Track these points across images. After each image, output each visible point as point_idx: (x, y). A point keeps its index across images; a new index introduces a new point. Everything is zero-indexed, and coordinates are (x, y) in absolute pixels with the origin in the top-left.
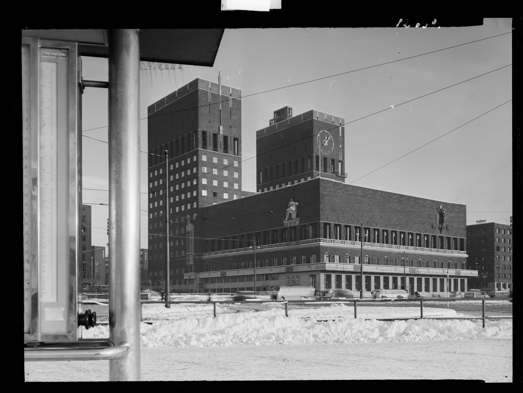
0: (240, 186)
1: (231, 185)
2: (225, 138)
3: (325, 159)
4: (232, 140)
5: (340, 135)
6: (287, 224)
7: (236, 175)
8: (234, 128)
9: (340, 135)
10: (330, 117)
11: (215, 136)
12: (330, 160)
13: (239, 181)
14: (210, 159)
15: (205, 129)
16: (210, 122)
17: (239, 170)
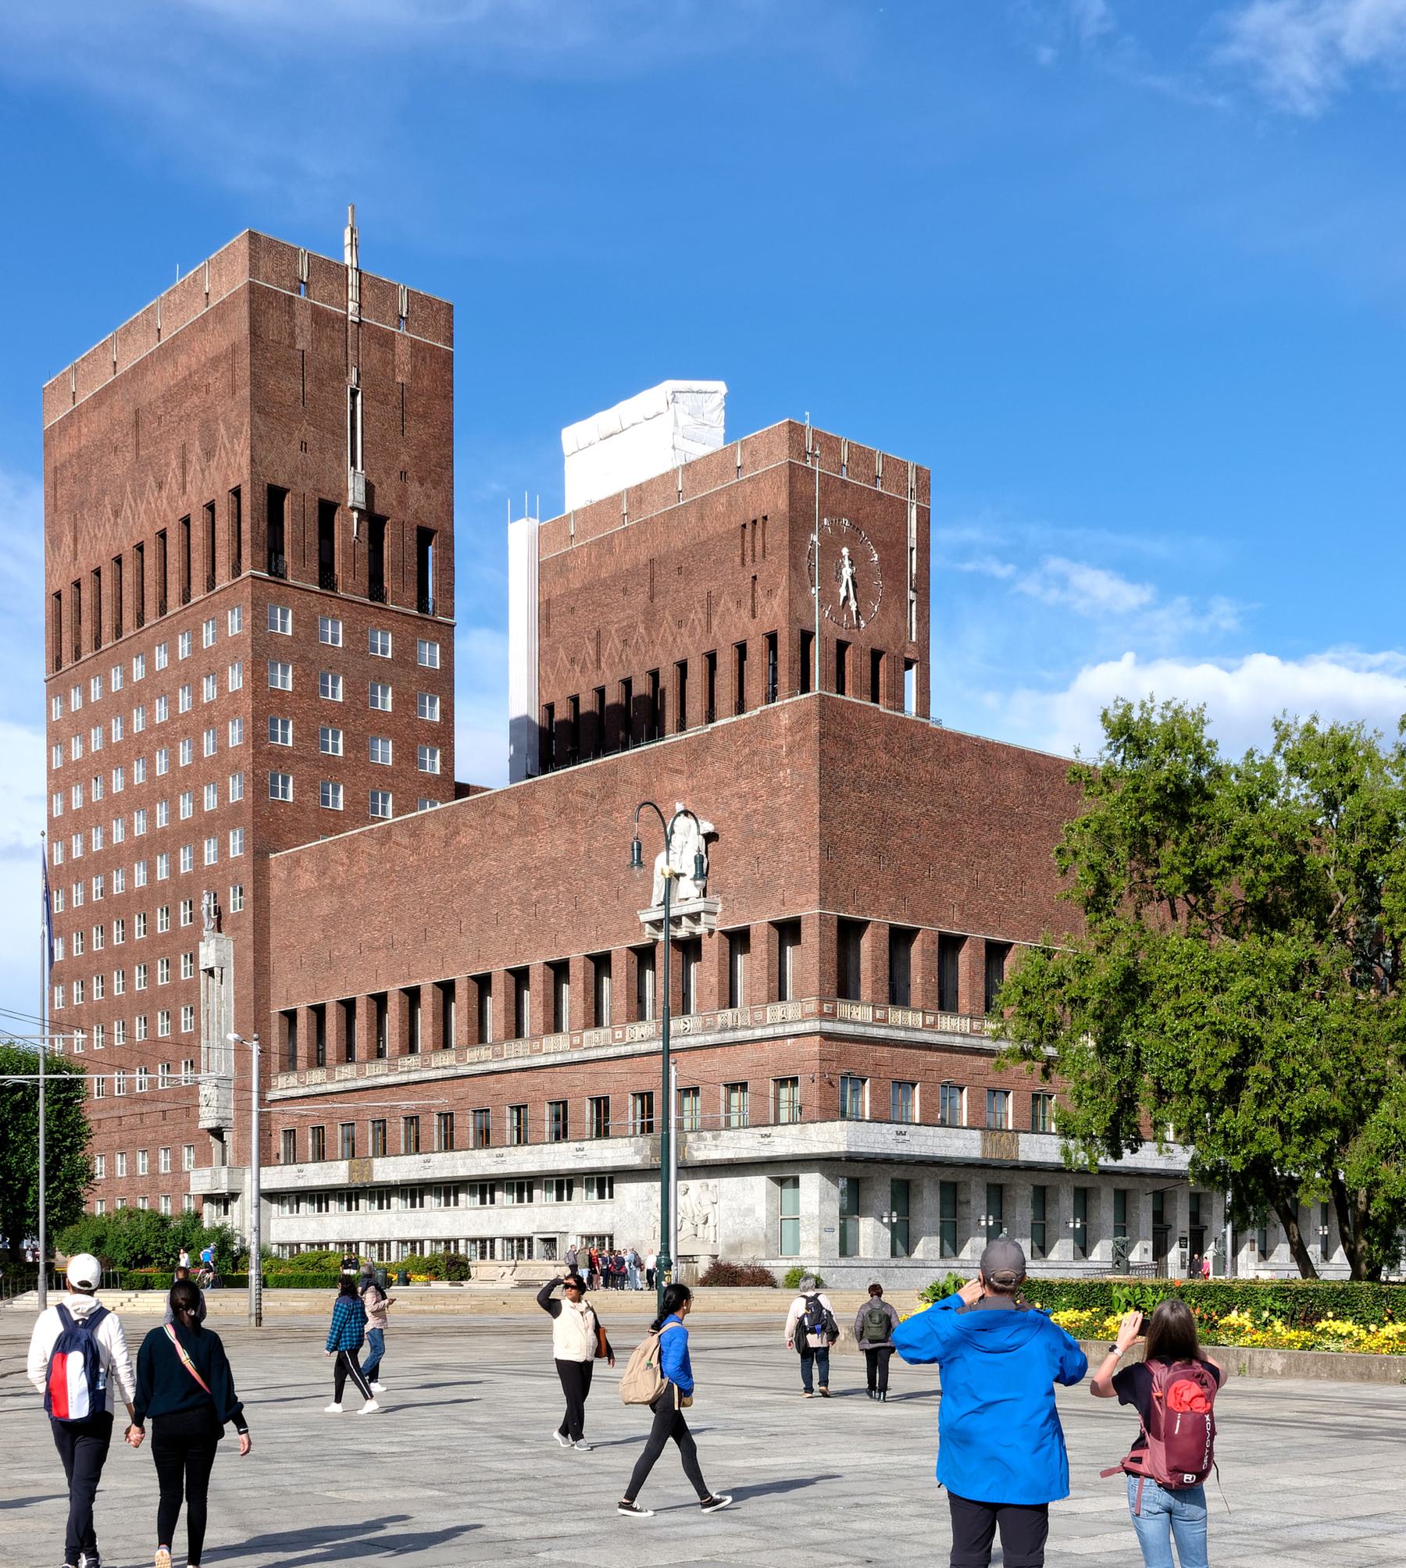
5: (912, 542)
9: (912, 542)
13: (443, 736)
17: (443, 683)
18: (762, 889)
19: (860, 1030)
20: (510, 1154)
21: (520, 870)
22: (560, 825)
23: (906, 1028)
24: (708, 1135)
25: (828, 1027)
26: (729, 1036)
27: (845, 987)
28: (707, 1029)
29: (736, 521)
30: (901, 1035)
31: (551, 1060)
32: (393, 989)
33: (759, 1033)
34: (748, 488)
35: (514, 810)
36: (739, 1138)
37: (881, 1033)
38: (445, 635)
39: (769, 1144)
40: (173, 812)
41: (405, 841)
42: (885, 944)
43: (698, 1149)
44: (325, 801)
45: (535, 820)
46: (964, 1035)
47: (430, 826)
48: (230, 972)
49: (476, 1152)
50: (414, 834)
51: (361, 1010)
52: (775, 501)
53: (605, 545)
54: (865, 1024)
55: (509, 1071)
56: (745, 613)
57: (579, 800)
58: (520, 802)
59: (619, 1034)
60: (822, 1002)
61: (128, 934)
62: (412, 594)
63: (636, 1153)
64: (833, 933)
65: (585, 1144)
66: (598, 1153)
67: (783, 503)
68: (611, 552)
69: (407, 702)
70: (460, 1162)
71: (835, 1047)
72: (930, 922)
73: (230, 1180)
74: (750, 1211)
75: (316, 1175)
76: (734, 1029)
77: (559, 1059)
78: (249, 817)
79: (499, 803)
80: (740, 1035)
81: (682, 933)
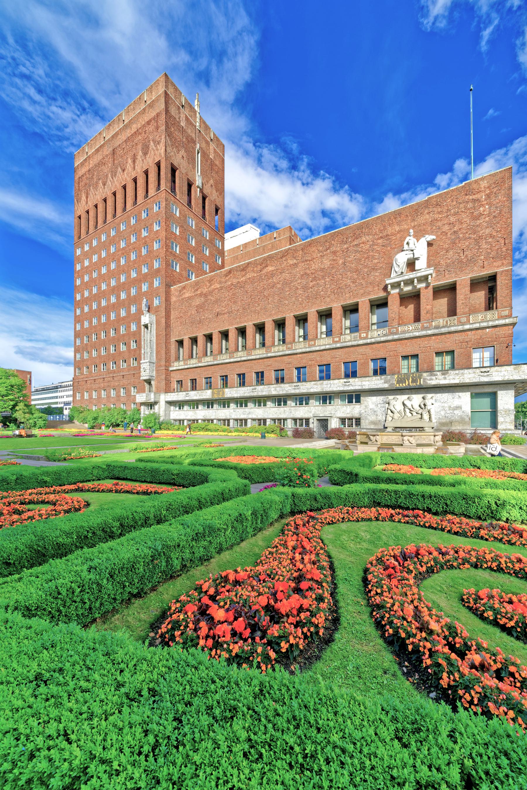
18: (461, 265)
20: (303, 385)
21: (302, 275)
22: (327, 254)
26: (443, 330)
31: (323, 348)
36: (463, 374)
39: (488, 375)
43: (431, 379)
55: (296, 354)
58: (302, 250)
63: (385, 383)
66: (360, 383)
70: (273, 389)
73: (155, 397)
75: (194, 395)
77: (328, 347)
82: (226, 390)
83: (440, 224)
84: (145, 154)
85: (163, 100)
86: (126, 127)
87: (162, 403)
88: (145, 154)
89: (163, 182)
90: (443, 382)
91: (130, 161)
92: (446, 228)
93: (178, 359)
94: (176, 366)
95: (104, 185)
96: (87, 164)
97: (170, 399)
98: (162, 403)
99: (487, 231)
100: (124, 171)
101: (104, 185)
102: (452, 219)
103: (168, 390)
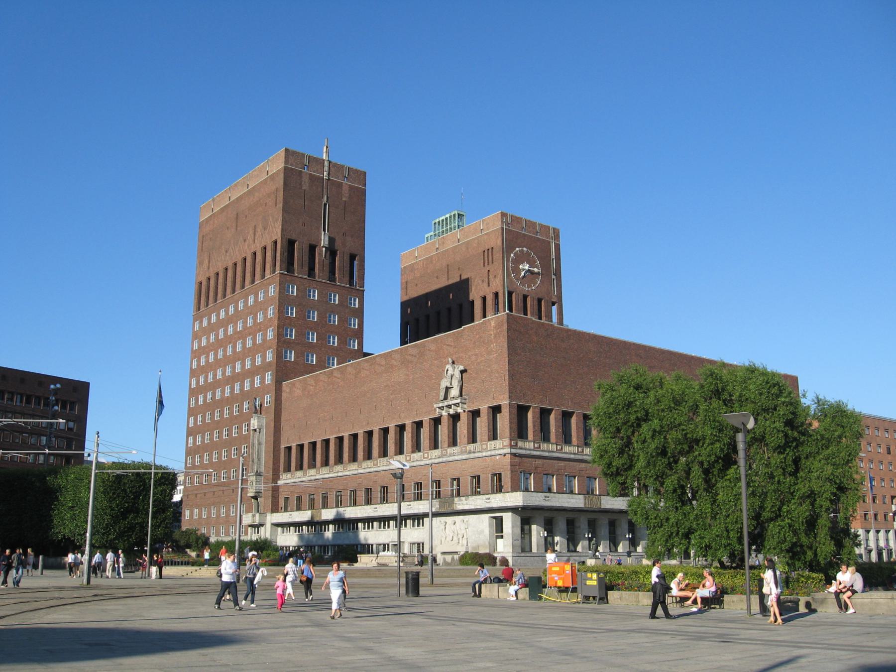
0: (361, 344)
1: (343, 342)
2: (332, 252)
3: (525, 297)
4: (347, 258)
6: (442, 408)
7: (354, 324)
8: (352, 237)
10: (531, 224)
11: (312, 248)
12: (536, 302)
13: (359, 334)
14: (304, 292)
15: (294, 237)
16: (304, 224)
17: (359, 313)
19: (528, 452)
23: (549, 452)
24: (463, 498)
25: (514, 451)
26: (472, 455)
27: (520, 432)
28: (462, 453)
29: (481, 250)
30: (547, 454)
32: (332, 437)
33: (484, 454)
34: (486, 237)
35: (384, 363)
37: (538, 453)
38: (361, 294)
40: (243, 365)
41: (339, 376)
42: (538, 415)
44: (308, 360)
45: (392, 366)
46: (575, 454)
47: (349, 369)
48: (264, 431)
49: (366, 507)
50: (342, 373)
51: (319, 446)
52: (496, 242)
53: (430, 260)
54: (530, 450)
56: (486, 284)
57: (410, 358)
59: (426, 455)
60: (511, 440)
61: (222, 415)
62: (347, 278)
64: (515, 411)
65: (411, 503)
67: (499, 242)
68: (431, 262)
69: (344, 321)
71: (517, 460)
72: (558, 406)
74: (482, 531)
76: (474, 452)
78: (274, 367)
79: (377, 359)
80: (477, 455)
81: (452, 411)
82: (323, 511)
83: (470, 354)
84: (265, 229)
85: (282, 176)
86: (250, 192)
87: (268, 526)
88: (265, 229)
89: (278, 264)
90: (467, 507)
91: (251, 232)
92: (474, 358)
93: (288, 469)
94: (285, 479)
95: (227, 252)
96: (211, 222)
97: (275, 521)
98: (268, 526)
99: (495, 367)
100: (245, 241)
101: (227, 252)
102: (477, 351)
103: (275, 509)
